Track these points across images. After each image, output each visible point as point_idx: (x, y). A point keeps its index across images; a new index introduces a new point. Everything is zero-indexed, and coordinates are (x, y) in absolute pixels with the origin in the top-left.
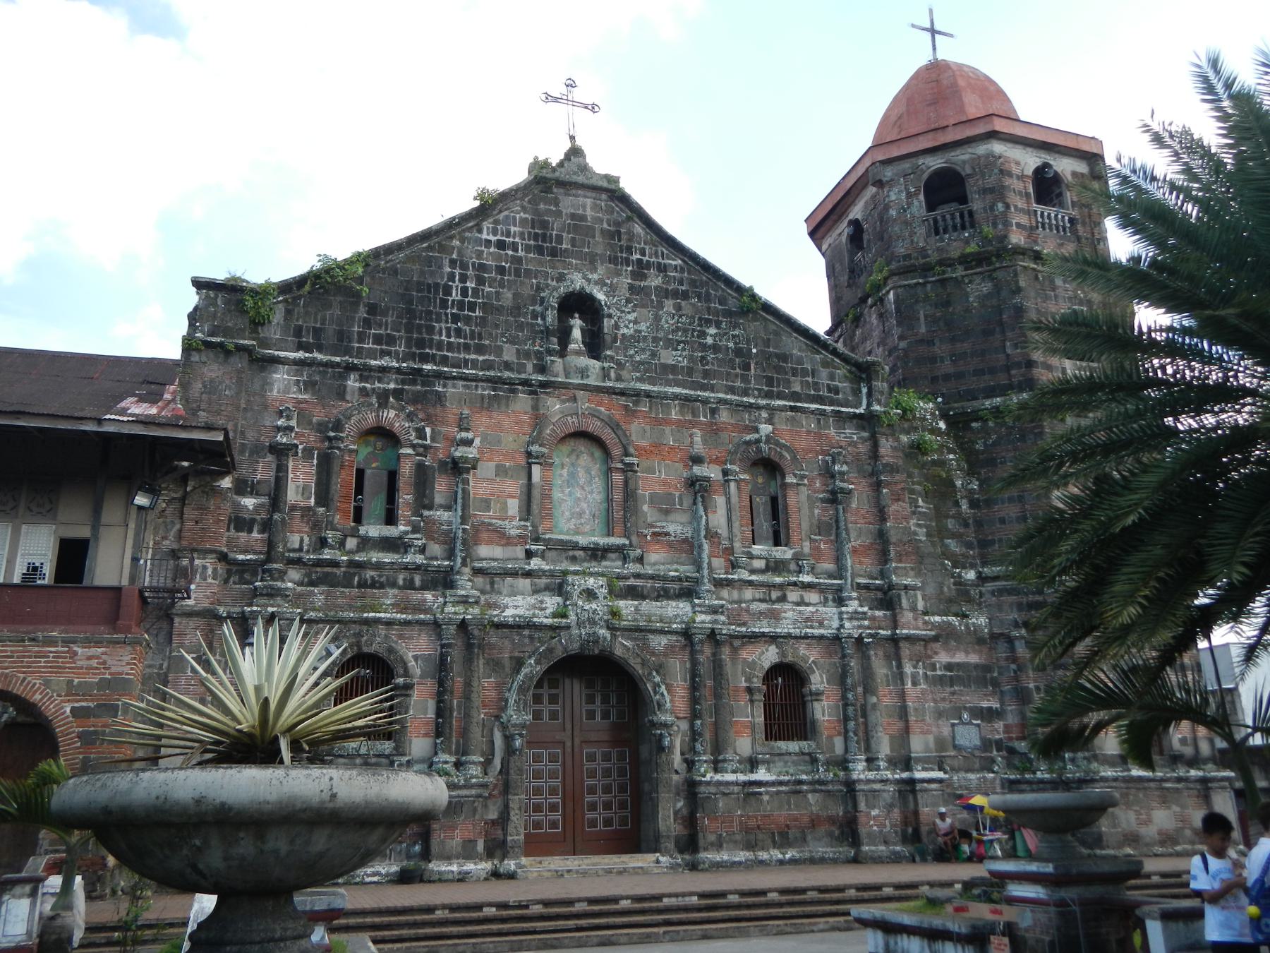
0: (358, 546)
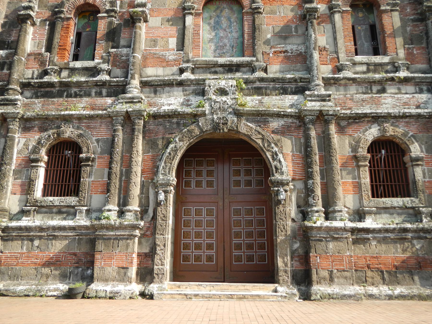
0: (69, 75)
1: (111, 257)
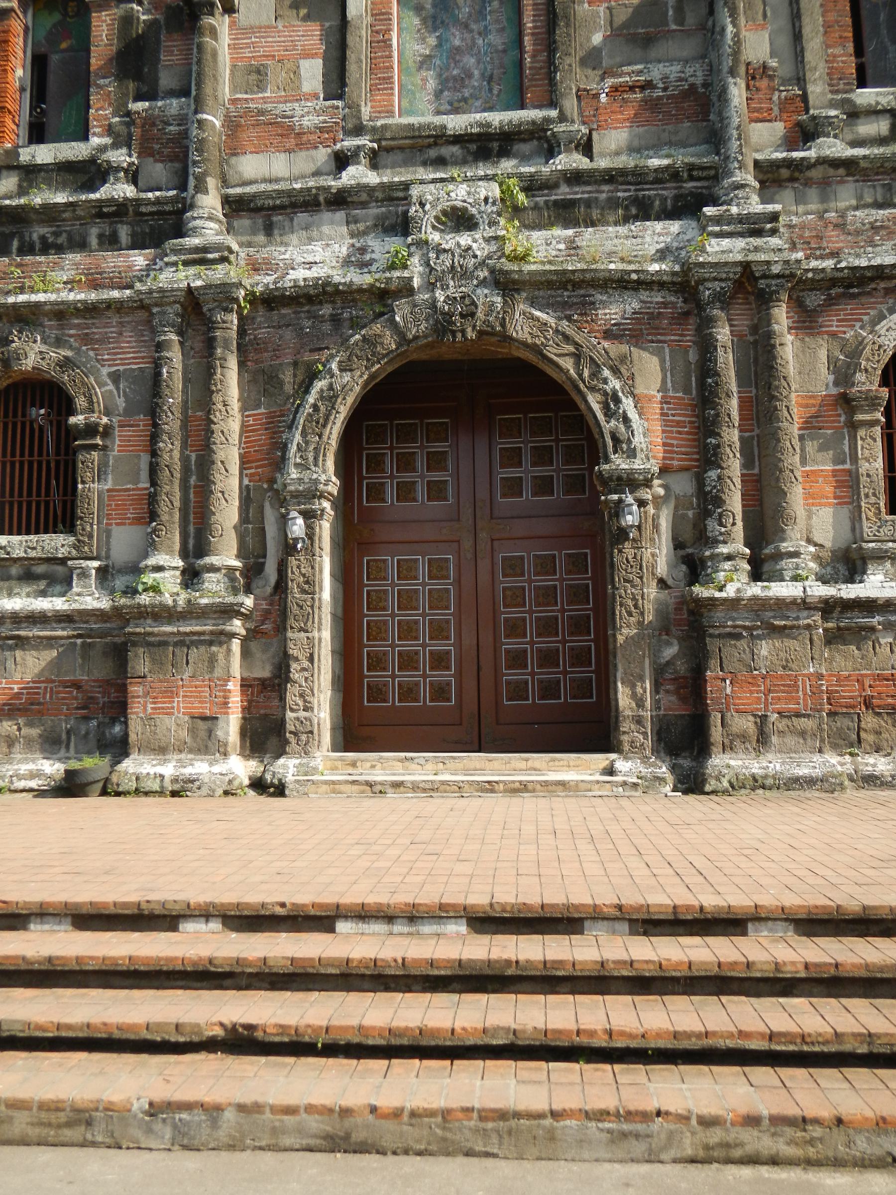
0: (20, 186)
1: (172, 692)
